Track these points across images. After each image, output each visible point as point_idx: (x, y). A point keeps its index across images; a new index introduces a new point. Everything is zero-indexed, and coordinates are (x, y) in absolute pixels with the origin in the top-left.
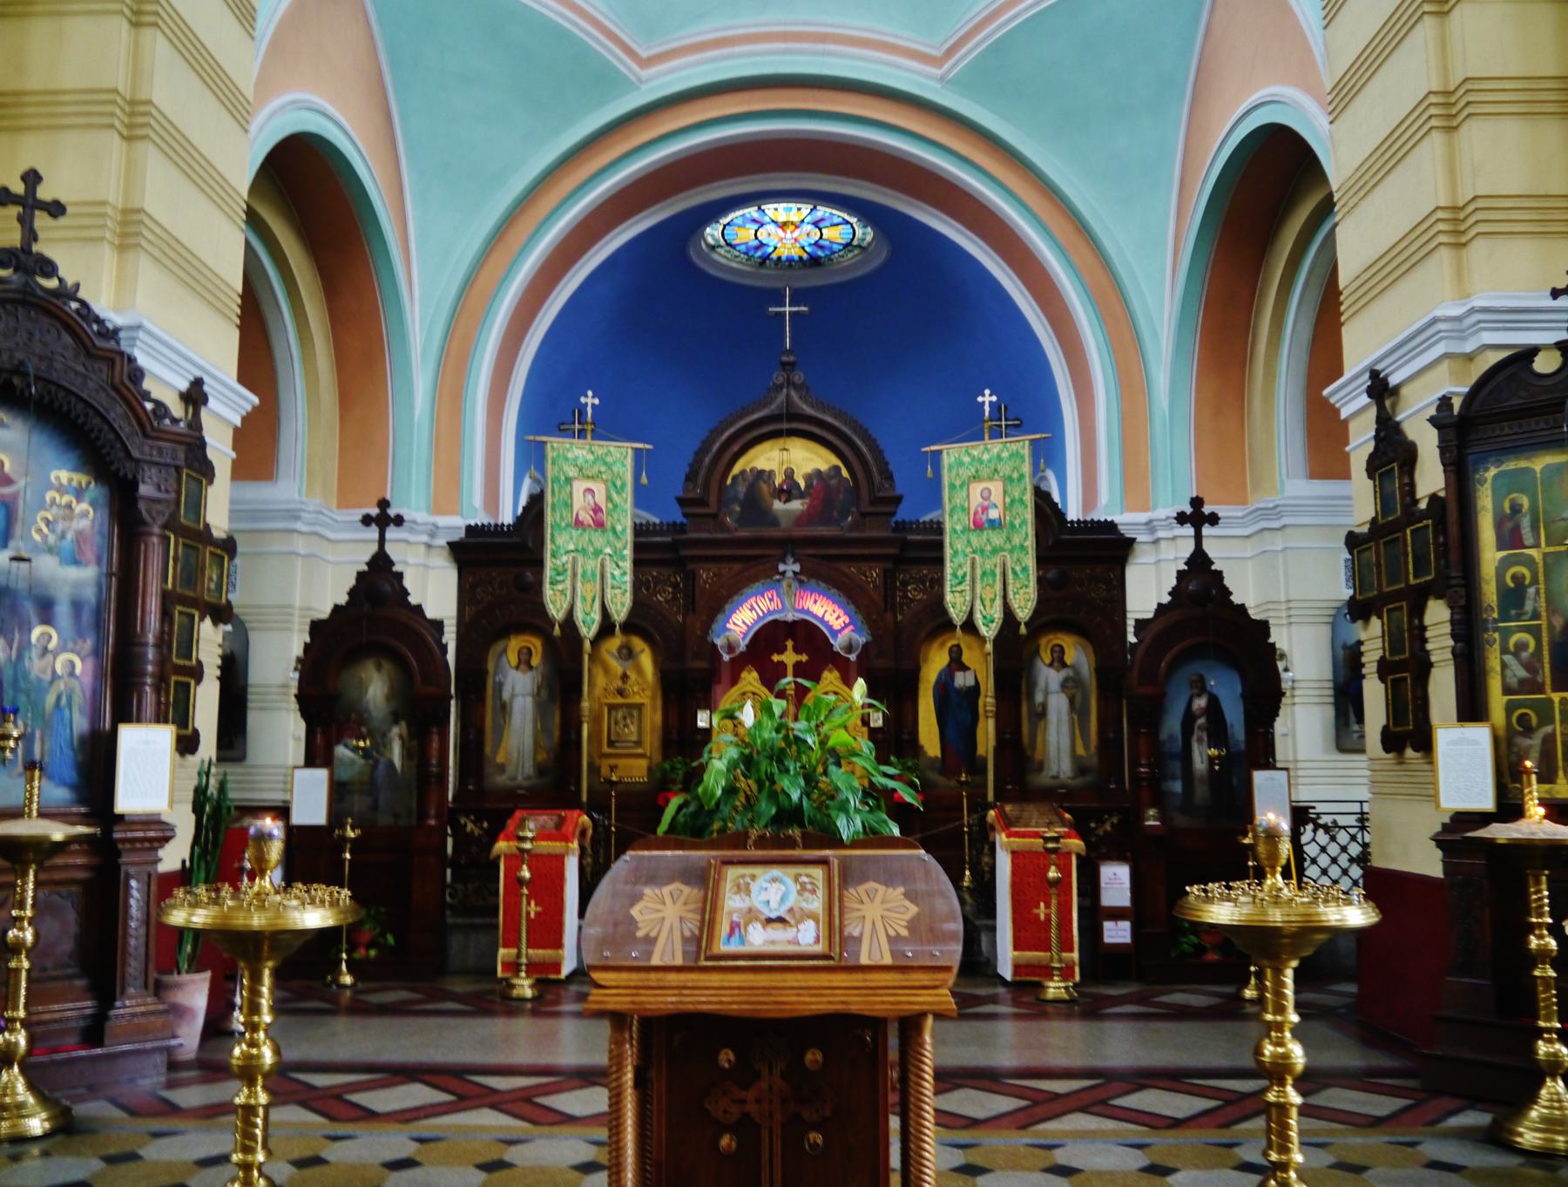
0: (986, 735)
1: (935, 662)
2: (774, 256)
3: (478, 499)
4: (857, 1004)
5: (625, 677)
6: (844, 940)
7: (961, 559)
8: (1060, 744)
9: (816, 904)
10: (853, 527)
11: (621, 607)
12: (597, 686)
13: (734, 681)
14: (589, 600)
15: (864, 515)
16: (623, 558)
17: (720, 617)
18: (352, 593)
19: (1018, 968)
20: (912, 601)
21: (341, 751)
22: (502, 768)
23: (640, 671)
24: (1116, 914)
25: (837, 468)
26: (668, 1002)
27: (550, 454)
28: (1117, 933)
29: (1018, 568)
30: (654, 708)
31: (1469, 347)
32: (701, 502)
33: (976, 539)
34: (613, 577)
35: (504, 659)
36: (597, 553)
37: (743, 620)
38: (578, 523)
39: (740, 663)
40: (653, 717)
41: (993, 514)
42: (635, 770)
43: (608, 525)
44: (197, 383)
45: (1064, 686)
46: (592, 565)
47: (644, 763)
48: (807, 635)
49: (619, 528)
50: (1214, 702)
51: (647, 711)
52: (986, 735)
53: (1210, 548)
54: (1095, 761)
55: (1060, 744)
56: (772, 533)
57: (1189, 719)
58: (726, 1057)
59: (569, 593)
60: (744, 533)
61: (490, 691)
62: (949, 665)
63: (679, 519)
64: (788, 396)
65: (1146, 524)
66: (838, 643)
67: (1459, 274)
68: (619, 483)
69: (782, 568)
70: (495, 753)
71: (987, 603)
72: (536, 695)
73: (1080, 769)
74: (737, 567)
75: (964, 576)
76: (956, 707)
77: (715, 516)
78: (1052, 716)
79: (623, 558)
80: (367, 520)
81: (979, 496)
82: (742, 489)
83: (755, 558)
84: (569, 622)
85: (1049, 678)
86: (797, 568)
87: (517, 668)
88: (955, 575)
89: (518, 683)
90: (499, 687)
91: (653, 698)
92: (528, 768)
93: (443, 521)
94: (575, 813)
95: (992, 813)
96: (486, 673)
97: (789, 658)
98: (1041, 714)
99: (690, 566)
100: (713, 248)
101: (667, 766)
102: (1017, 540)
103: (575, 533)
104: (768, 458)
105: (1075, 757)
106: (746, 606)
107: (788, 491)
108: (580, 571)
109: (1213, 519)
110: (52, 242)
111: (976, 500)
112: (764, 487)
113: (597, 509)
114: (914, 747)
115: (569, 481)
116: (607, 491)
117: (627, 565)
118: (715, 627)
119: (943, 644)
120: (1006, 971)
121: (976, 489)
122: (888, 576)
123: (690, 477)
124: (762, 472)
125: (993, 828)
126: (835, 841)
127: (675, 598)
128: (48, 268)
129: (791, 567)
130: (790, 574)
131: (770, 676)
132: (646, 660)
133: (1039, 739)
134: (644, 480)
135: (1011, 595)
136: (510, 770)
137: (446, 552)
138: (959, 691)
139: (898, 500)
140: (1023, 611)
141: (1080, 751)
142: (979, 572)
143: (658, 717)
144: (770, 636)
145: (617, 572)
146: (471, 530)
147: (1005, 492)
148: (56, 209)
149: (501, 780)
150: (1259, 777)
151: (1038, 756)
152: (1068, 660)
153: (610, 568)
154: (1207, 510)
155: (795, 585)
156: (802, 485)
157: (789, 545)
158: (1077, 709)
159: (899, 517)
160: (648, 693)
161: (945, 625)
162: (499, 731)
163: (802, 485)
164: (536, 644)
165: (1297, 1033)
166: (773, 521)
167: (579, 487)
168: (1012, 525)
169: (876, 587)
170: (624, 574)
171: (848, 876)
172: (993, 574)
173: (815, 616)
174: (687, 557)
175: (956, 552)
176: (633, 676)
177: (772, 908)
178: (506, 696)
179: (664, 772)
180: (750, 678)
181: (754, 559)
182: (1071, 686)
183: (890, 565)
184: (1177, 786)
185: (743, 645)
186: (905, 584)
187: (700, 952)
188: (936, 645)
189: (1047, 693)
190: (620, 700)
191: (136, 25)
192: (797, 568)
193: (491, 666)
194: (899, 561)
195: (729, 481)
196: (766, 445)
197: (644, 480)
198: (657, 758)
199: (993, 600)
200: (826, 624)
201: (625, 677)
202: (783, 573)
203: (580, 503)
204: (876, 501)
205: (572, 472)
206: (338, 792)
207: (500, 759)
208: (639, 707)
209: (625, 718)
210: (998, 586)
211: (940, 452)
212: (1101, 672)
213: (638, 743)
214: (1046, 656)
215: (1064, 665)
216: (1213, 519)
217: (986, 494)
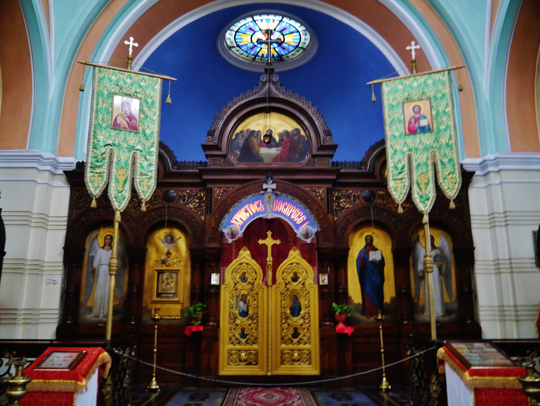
0: (389, 291)
2: (260, 54)
5: (168, 253)
7: (399, 156)
10: (307, 164)
14: (122, 183)
15: (314, 156)
16: (150, 153)
17: (227, 216)
20: (343, 208)
22: (90, 310)
23: (178, 250)
25: (297, 130)
29: (445, 160)
30: (186, 273)
32: (217, 147)
34: (143, 168)
35: (96, 243)
37: (240, 218)
38: (116, 126)
39: (239, 244)
40: (185, 278)
41: (424, 123)
43: (140, 129)
47: (178, 307)
49: (148, 132)
51: (181, 275)
52: (389, 291)
54: (455, 306)
56: (260, 166)
59: (105, 175)
60: (243, 166)
61: (86, 262)
62: (365, 247)
63: (204, 159)
64: (269, 87)
65: (480, 164)
66: (299, 233)
68: (150, 101)
69: (265, 186)
70: (87, 300)
71: (423, 186)
73: (447, 311)
74: (237, 186)
75: (403, 167)
76: (370, 272)
77: (225, 156)
79: (150, 153)
82: (241, 142)
83: (249, 180)
84: (104, 196)
86: (274, 186)
87: (103, 247)
88: (396, 167)
90: (92, 259)
91: (186, 266)
93: (61, 159)
94: (96, 351)
95: (441, 350)
96: (84, 250)
97: (269, 242)
99: (209, 186)
100: (230, 48)
101: (191, 309)
103: (113, 133)
104: (258, 124)
105: (444, 304)
106: (243, 210)
108: (115, 160)
111: (410, 113)
112: (255, 141)
113: (131, 117)
114: (343, 296)
116: (141, 105)
118: (223, 222)
119: (361, 235)
122: (329, 192)
124: (253, 132)
125: (442, 362)
127: (200, 206)
129: (270, 186)
130: (269, 190)
131: (259, 254)
132: (182, 243)
133: (421, 292)
134: (169, 100)
135: (441, 180)
136: (95, 311)
137: (64, 178)
138: (374, 262)
139: (334, 148)
141: (447, 300)
142: (414, 164)
143: (188, 278)
144: (258, 228)
145: (145, 163)
147: (431, 107)
149: (90, 317)
151: (421, 303)
152: (437, 244)
153: (140, 160)
155: (274, 196)
156: (277, 139)
157: (269, 173)
158: (444, 274)
159: (334, 159)
160: (182, 263)
162: (91, 287)
163: (277, 139)
168: (439, 131)
169: (322, 199)
170: (150, 165)
172: (426, 164)
173: (285, 216)
175: (396, 151)
176: (174, 253)
178: (95, 265)
179: (190, 313)
181: (249, 180)
182: (439, 258)
183: (330, 186)
185: (240, 234)
186: (338, 198)
188: (357, 235)
190: (164, 268)
192: (274, 186)
193: (87, 247)
194: (335, 184)
195: (234, 137)
196: (256, 117)
197: (169, 100)
198: (187, 304)
199: (427, 184)
200: (292, 220)
201: (168, 253)
202: (266, 189)
204: (321, 148)
208: (177, 272)
209: (167, 279)
210: (431, 175)
211: (380, 84)
212: (456, 251)
213: (175, 294)
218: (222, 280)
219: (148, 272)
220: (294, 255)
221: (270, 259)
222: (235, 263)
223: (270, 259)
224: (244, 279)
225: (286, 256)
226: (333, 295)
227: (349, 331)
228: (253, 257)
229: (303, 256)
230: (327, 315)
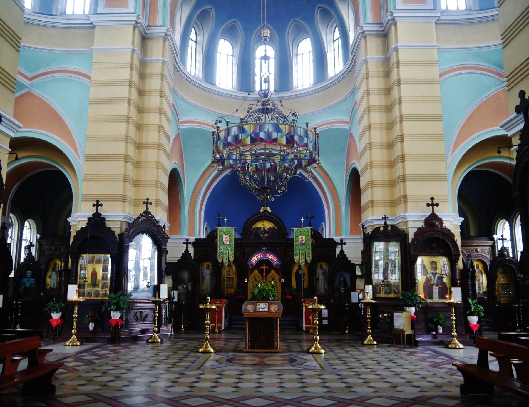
1: (296, 268)
3: (198, 233)
4: (271, 316)
5: (229, 271)
6: (270, 311)
8: (322, 285)
9: (267, 307)
11: (232, 259)
12: (224, 273)
13: (253, 272)
18: (181, 257)
19: (306, 328)
21: (179, 287)
22: (203, 290)
23: (232, 270)
24: (325, 319)
25: (274, 227)
26: (251, 316)
27: (218, 230)
28: (325, 322)
31: (373, 224)
33: (300, 247)
36: (227, 249)
37: (254, 259)
40: (235, 280)
41: (304, 242)
42: (232, 291)
44: (165, 225)
45: (323, 273)
46: (227, 252)
47: (233, 290)
48: (268, 262)
50: (345, 279)
53: (344, 249)
55: (322, 285)
57: (340, 282)
58: (257, 323)
66: (274, 264)
67: (372, 212)
70: (202, 287)
72: (210, 275)
78: (320, 280)
80: (184, 243)
81: (301, 237)
82: (254, 231)
85: (320, 272)
89: (207, 273)
90: (202, 273)
92: (209, 290)
97: (264, 267)
98: (318, 279)
102: (308, 247)
104: (260, 225)
105: (325, 289)
109: (345, 244)
110: (151, 209)
111: (300, 239)
112: (259, 231)
115: (222, 235)
117: (233, 251)
120: (304, 329)
121: (300, 237)
123: (243, 229)
126: (269, 300)
128: (150, 213)
129: (265, 248)
131: (261, 272)
132: (234, 268)
139: (287, 234)
140: (309, 260)
141: (326, 287)
144: (260, 262)
148: (151, 204)
149: (203, 293)
150: (353, 293)
153: (230, 252)
154: (344, 242)
157: (264, 244)
161: (295, 262)
164: (210, 264)
165: (318, 320)
166: (261, 238)
167: (224, 236)
171: (271, 304)
174: (243, 248)
177: (262, 307)
180: (256, 272)
184: (338, 295)
187: (255, 311)
189: (319, 275)
191: (157, 168)
193: (201, 268)
196: (259, 222)
201: (229, 271)
203: (224, 239)
205: (223, 234)
206: (179, 295)
207: (203, 288)
208: (232, 278)
213: (232, 285)
214: (319, 267)
215: (323, 269)
216: (345, 244)
217: (302, 238)
218: (248, 280)
219: (222, 277)
220: (273, 272)
221: (264, 273)
222: (252, 275)
223: (264, 273)
224: (256, 280)
225: (270, 272)
226: (286, 286)
227: (290, 297)
228: (259, 273)
229: (276, 272)
230: (283, 292)
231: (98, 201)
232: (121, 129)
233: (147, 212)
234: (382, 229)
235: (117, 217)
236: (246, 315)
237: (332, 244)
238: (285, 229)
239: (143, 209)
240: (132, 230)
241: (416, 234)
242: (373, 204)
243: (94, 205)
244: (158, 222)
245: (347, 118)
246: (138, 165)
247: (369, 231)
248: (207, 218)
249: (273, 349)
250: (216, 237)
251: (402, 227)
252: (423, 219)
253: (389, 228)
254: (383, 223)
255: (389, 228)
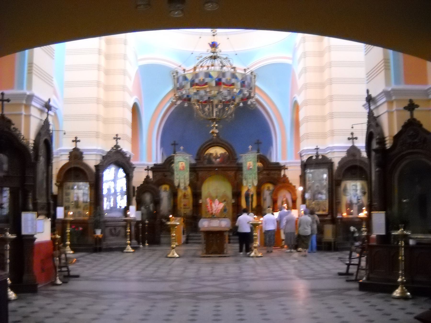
11: (188, 183)
12: (180, 194)
25: (225, 153)
41: (251, 167)
52: (255, 204)
56: (214, 166)
81: (249, 162)
82: (207, 157)
89: (164, 194)
98: (265, 200)
107: (216, 157)
110: (120, 143)
122: (236, 173)
140: (256, 183)
146: (155, 165)
148: (119, 139)
231: (76, 138)
232: (93, 75)
233: (117, 146)
234: (314, 158)
235: (93, 151)
236: (202, 229)
237: (279, 168)
238: (236, 155)
239: (114, 143)
240: (106, 161)
241: (340, 163)
242: (308, 136)
243: (73, 141)
244: (126, 154)
245: (290, 56)
246: (107, 105)
247: (305, 159)
248: (163, 144)
249: (224, 254)
250: (173, 163)
251: (329, 156)
252: (346, 150)
253: (320, 157)
254: (315, 153)
255: (320, 157)
